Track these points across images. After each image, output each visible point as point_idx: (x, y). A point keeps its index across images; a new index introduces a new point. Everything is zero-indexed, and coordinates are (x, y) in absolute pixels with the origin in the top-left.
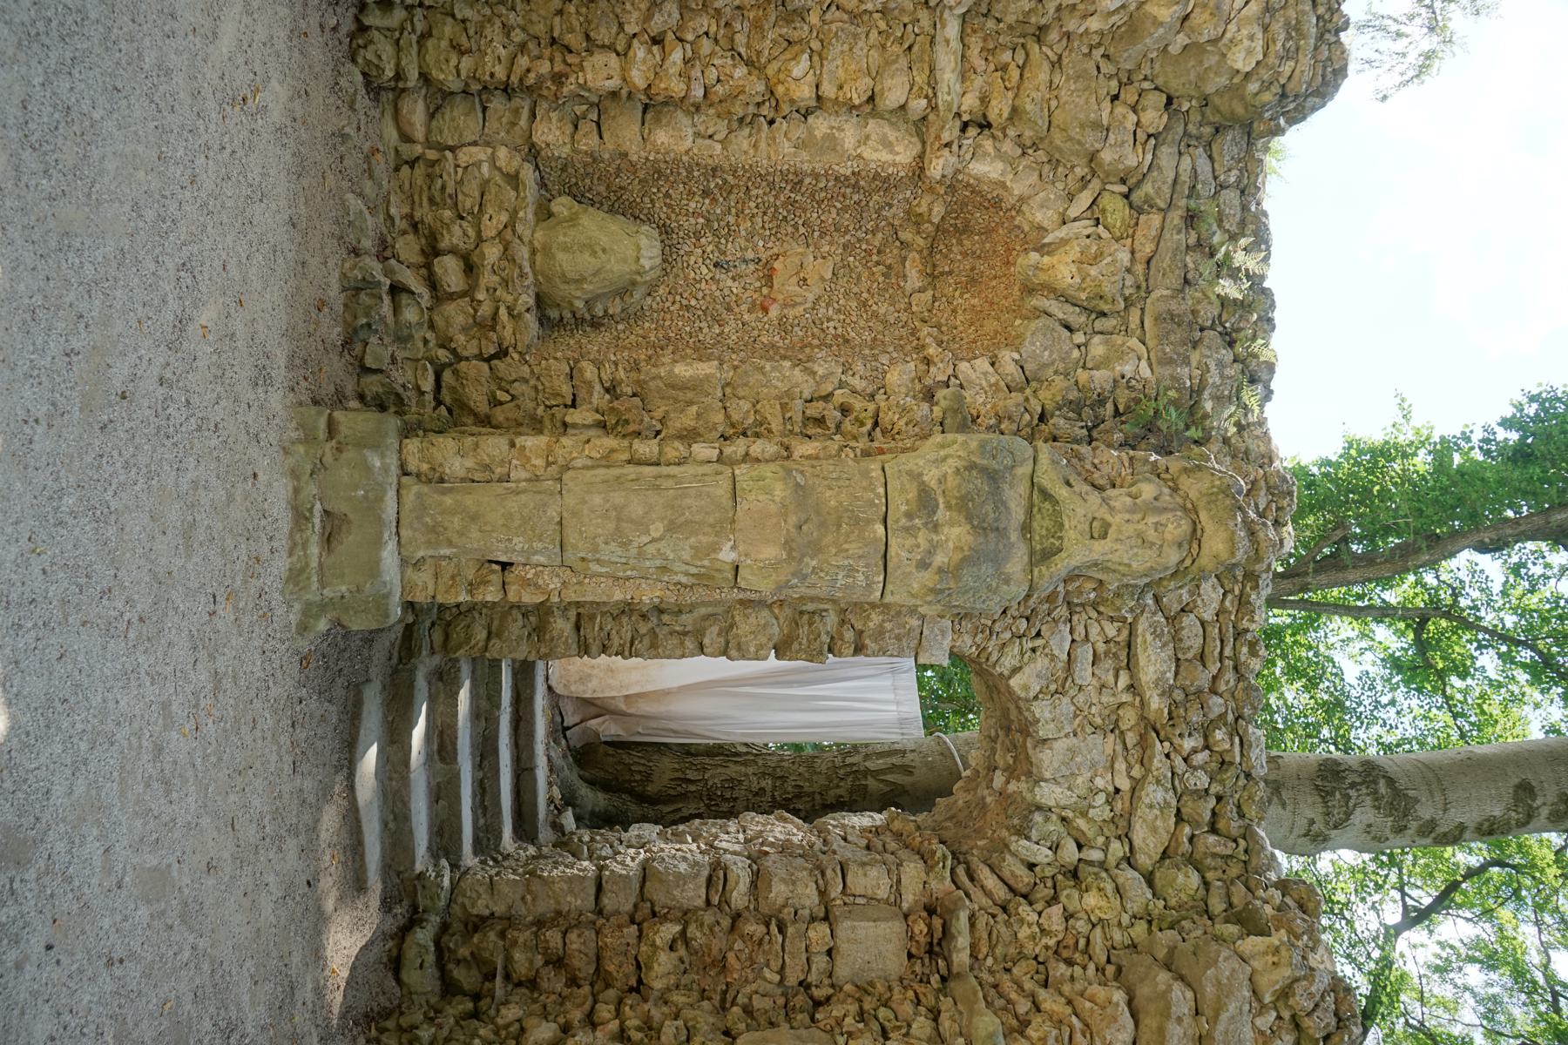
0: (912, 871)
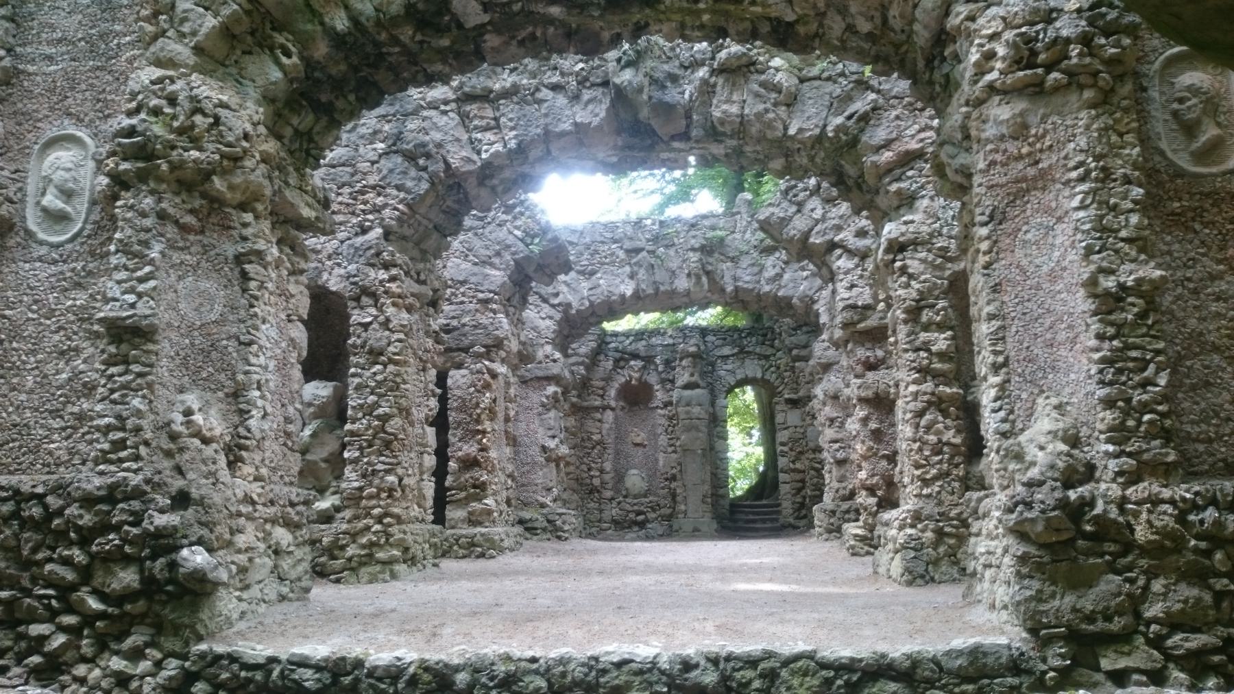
0: (778, 407)
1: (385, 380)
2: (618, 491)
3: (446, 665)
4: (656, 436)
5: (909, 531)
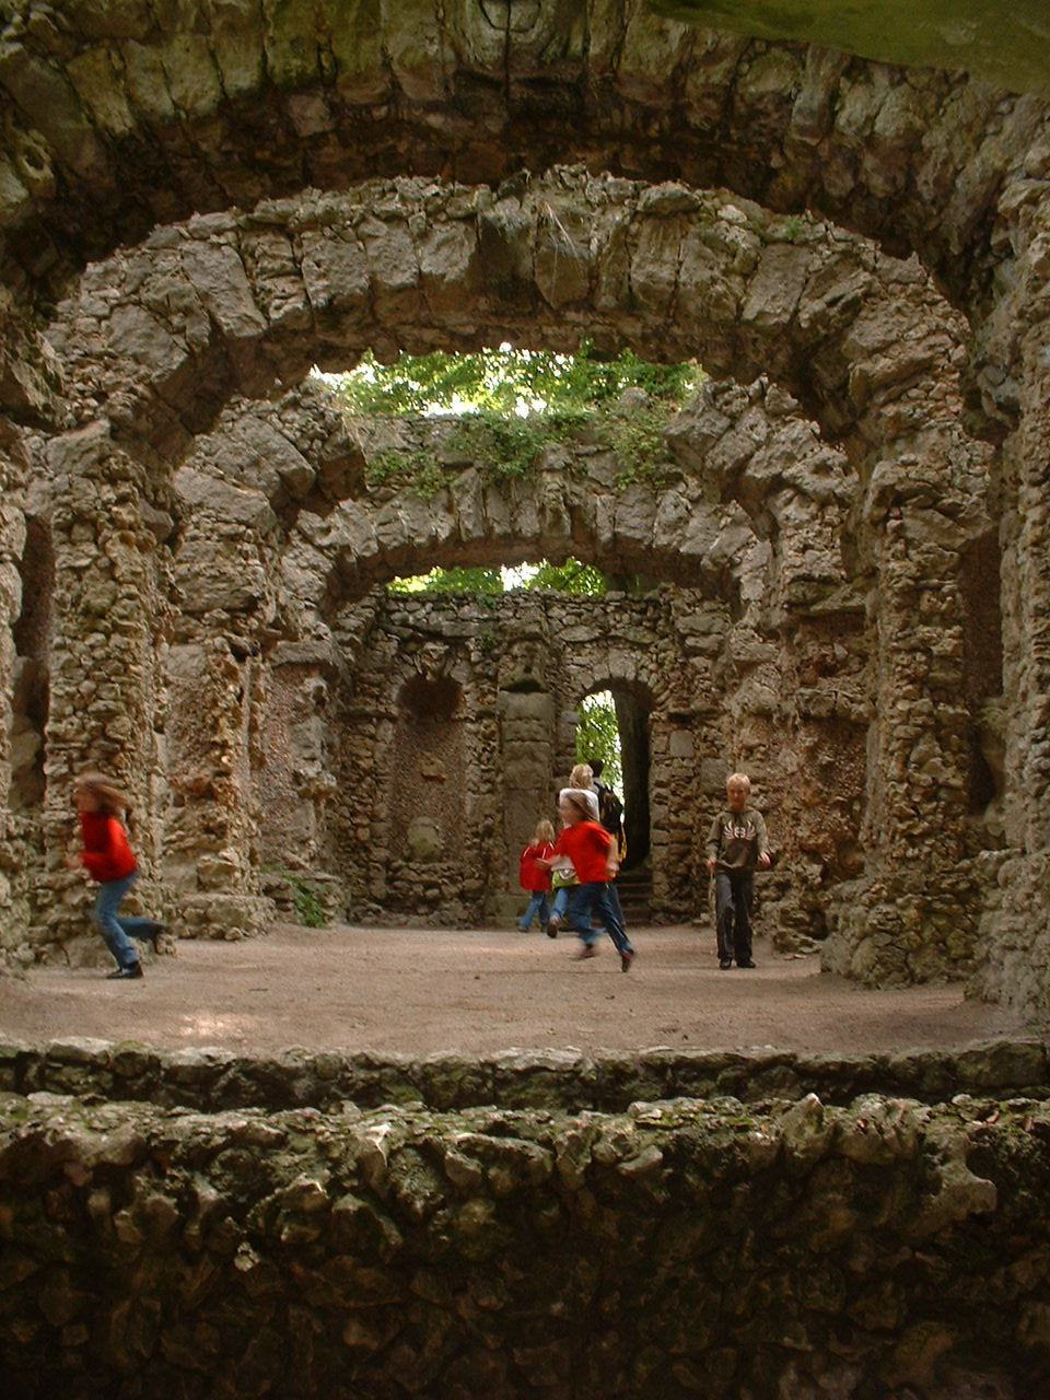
1: (108, 657)
2: (397, 851)
3: (279, 1069)
4: (462, 765)
5: (885, 908)
